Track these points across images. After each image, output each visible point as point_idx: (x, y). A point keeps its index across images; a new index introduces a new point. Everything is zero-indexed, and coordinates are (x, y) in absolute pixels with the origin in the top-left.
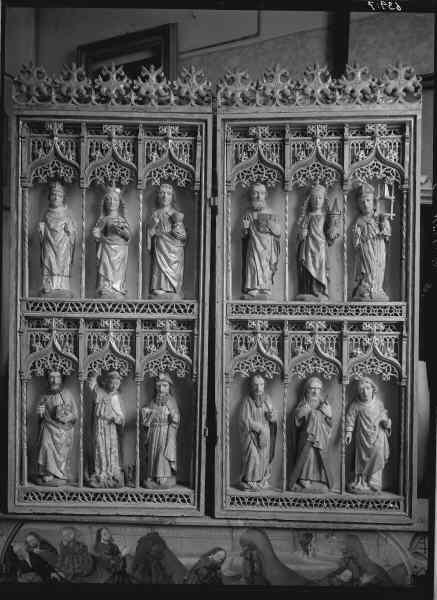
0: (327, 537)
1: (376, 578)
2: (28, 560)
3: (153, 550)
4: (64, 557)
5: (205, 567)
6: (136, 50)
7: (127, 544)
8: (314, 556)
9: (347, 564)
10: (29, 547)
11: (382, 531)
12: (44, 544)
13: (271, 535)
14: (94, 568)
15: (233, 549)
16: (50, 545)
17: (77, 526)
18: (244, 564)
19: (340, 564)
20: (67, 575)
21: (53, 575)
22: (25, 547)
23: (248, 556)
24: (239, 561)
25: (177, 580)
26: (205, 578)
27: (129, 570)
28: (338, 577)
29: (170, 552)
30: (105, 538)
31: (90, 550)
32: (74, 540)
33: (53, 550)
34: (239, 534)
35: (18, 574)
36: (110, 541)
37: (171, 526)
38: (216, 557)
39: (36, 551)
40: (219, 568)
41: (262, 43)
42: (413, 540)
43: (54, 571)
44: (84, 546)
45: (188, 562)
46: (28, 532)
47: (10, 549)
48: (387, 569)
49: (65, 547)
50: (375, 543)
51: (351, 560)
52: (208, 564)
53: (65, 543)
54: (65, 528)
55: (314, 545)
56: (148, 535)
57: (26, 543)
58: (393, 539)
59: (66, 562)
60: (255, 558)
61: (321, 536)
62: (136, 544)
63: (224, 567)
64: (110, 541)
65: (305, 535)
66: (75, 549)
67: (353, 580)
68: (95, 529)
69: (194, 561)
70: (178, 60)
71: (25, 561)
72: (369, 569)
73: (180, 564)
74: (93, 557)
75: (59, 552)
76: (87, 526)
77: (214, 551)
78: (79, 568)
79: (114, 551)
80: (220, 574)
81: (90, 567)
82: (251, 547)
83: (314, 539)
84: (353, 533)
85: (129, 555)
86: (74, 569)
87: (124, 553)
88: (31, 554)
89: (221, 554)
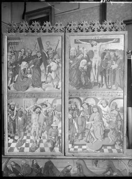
0: (103, 161)
1: (118, 174)
2: (12, 170)
3: (49, 166)
4: (22, 169)
5: (66, 171)
6: (41, 14)
8: (99, 167)
10: (12, 166)
11: (120, 159)
12: (16, 165)
13: (85, 160)
14: (32, 172)
16: (18, 165)
17: (27, 159)
18: (78, 170)
19: (107, 169)
20: (23, 174)
24: (76, 169)
25: (57, 175)
27: (42, 172)
28: (106, 173)
30: (35, 163)
32: (25, 163)
33: (19, 166)
34: (76, 161)
36: (37, 164)
37: (55, 158)
38: (69, 168)
39: (14, 167)
40: (70, 171)
41: (80, 11)
42: (129, 162)
43: (20, 173)
44: (29, 165)
45: (60, 170)
46: (12, 161)
47: (6, 166)
48: (121, 171)
49: (23, 166)
50: (117, 163)
51: (110, 168)
52: (66, 170)
54: (23, 160)
55: (99, 164)
56: (48, 161)
57: (11, 164)
60: (81, 168)
61: (101, 161)
63: (71, 171)
64: (37, 164)
65: (96, 161)
67: (111, 174)
68: (32, 160)
69: (63, 169)
70: (54, 16)
72: (116, 171)
73: (57, 170)
74: (31, 168)
75: (21, 167)
76: (29, 159)
77: (69, 166)
79: (38, 166)
80: (70, 173)
81: (30, 172)
82: (80, 165)
84: (110, 160)
87: (41, 167)
88: (13, 168)
89: (70, 167)
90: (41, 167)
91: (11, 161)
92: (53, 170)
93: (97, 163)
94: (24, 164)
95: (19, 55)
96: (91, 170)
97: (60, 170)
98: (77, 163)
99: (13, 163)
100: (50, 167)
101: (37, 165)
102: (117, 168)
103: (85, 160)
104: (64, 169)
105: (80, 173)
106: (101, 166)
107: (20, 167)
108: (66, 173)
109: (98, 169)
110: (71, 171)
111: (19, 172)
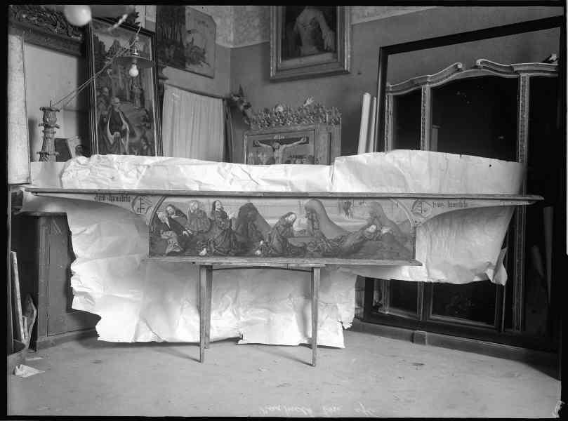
0: (360, 204)
1: (391, 230)
2: (168, 223)
4: (191, 221)
7: (232, 213)
8: (352, 215)
9: (373, 222)
10: (168, 214)
12: (178, 212)
14: (211, 227)
15: (301, 213)
16: (182, 213)
20: (193, 232)
21: (184, 232)
22: (166, 214)
23: (310, 217)
24: (305, 221)
26: (283, 232)
27: (233, 228)
29: (260, 216)
30: (218, 207)
31: (208, 215)
32: (198, 209)
33: (185, 216)
34: (305, 202)
35: (161, 231)
36: (222, 209)
38: (290, 219)
39: (173, 217)
40: (292, 226)
43: (185, 230)
44: (205, 213)
45: (272, 222)
47: (155, 216)
48: (397, 224)
49: (192, 214)
51: (376, 218)
53: (192, 211)
57: (167, 211)
58: (401, 204)
59: (192, 224)
61: (357, 202)
62: (238, 211)
63: (295, 225)
64: (222, 209)
66: (199, 214)
67: (377, 231)
68: (212, 200)
69: (277, 221)
71: (165, 223)
72: (388, 224)
78: (201, 227)
79: (224, 216)
81: (208, 227)
83: (352, 206)
85: (233, 218)
86: (198, 229)
88: (170, 219)
89: (293, 216)
90: (230, 218)
91: (166, 203)
92: (255, 223)
93: (348, 208)
94: (194, 211)
95: (177, 96)
96: (338, 224)
97: (272, 222)
98: (306, 208)
99: (170, 208)
100: (249, 216)
101: (222, 211)
102: (389, 216)
103: (323, 201)
104: (279, 222)
105: (313, 228)
106: (357, 213)
107: (186, 217)
108: (283, 228)
109: (349, 220)
110: (294, 225)
111: (182, 227)
